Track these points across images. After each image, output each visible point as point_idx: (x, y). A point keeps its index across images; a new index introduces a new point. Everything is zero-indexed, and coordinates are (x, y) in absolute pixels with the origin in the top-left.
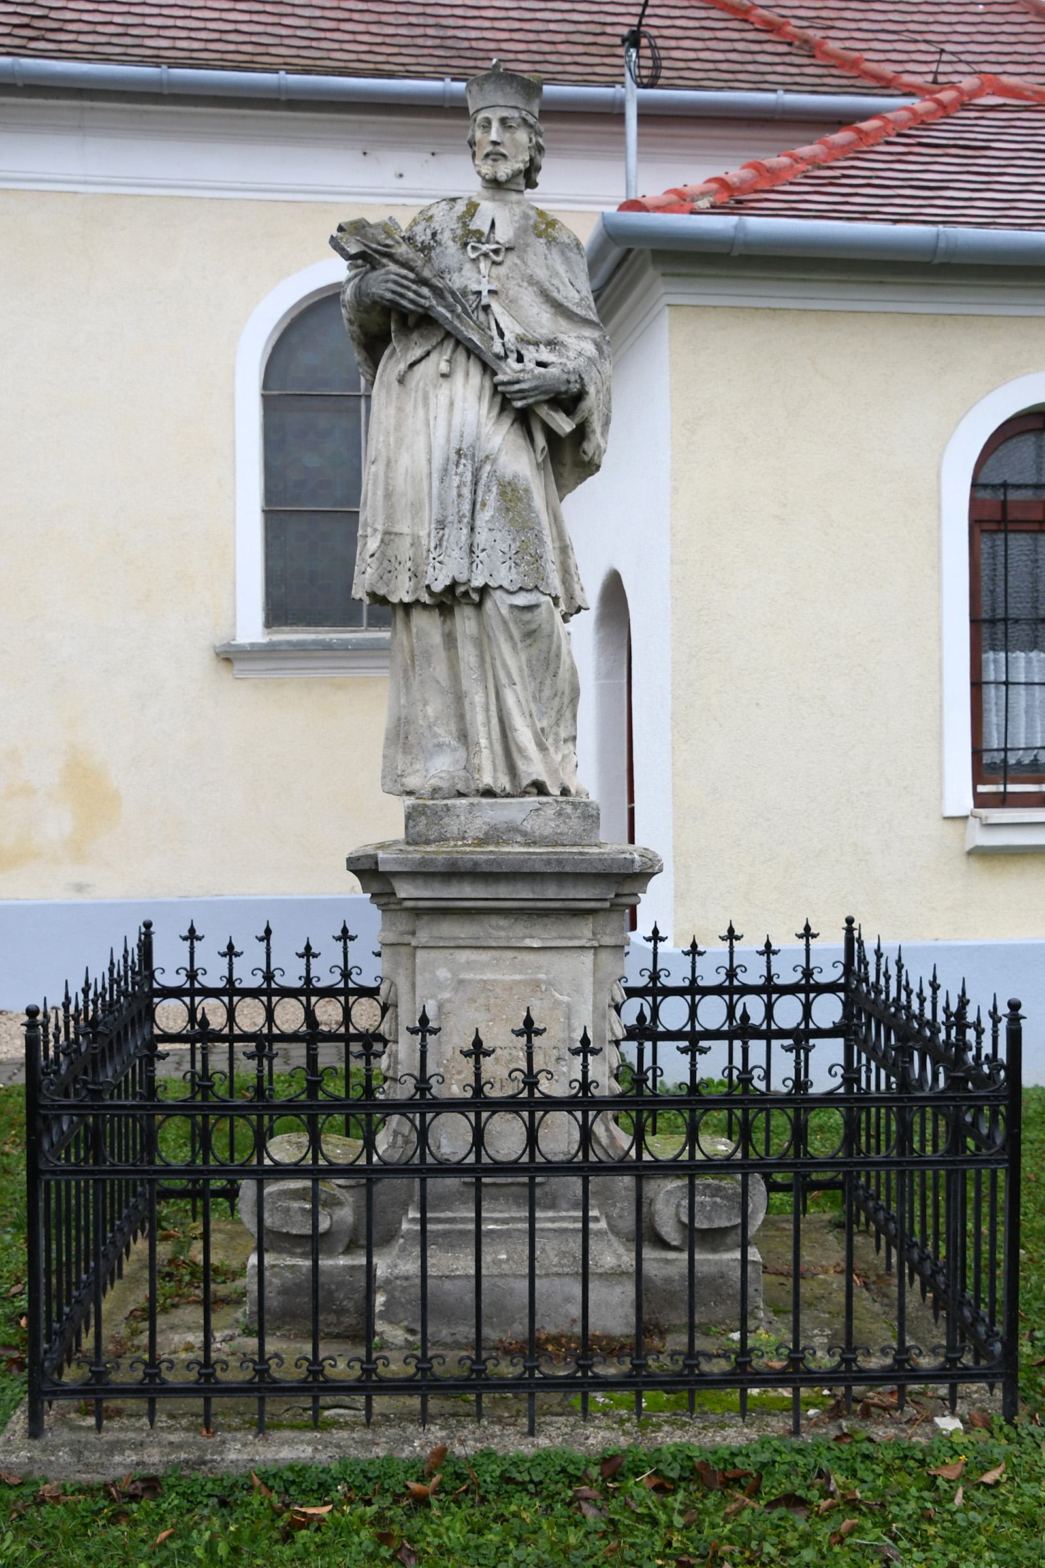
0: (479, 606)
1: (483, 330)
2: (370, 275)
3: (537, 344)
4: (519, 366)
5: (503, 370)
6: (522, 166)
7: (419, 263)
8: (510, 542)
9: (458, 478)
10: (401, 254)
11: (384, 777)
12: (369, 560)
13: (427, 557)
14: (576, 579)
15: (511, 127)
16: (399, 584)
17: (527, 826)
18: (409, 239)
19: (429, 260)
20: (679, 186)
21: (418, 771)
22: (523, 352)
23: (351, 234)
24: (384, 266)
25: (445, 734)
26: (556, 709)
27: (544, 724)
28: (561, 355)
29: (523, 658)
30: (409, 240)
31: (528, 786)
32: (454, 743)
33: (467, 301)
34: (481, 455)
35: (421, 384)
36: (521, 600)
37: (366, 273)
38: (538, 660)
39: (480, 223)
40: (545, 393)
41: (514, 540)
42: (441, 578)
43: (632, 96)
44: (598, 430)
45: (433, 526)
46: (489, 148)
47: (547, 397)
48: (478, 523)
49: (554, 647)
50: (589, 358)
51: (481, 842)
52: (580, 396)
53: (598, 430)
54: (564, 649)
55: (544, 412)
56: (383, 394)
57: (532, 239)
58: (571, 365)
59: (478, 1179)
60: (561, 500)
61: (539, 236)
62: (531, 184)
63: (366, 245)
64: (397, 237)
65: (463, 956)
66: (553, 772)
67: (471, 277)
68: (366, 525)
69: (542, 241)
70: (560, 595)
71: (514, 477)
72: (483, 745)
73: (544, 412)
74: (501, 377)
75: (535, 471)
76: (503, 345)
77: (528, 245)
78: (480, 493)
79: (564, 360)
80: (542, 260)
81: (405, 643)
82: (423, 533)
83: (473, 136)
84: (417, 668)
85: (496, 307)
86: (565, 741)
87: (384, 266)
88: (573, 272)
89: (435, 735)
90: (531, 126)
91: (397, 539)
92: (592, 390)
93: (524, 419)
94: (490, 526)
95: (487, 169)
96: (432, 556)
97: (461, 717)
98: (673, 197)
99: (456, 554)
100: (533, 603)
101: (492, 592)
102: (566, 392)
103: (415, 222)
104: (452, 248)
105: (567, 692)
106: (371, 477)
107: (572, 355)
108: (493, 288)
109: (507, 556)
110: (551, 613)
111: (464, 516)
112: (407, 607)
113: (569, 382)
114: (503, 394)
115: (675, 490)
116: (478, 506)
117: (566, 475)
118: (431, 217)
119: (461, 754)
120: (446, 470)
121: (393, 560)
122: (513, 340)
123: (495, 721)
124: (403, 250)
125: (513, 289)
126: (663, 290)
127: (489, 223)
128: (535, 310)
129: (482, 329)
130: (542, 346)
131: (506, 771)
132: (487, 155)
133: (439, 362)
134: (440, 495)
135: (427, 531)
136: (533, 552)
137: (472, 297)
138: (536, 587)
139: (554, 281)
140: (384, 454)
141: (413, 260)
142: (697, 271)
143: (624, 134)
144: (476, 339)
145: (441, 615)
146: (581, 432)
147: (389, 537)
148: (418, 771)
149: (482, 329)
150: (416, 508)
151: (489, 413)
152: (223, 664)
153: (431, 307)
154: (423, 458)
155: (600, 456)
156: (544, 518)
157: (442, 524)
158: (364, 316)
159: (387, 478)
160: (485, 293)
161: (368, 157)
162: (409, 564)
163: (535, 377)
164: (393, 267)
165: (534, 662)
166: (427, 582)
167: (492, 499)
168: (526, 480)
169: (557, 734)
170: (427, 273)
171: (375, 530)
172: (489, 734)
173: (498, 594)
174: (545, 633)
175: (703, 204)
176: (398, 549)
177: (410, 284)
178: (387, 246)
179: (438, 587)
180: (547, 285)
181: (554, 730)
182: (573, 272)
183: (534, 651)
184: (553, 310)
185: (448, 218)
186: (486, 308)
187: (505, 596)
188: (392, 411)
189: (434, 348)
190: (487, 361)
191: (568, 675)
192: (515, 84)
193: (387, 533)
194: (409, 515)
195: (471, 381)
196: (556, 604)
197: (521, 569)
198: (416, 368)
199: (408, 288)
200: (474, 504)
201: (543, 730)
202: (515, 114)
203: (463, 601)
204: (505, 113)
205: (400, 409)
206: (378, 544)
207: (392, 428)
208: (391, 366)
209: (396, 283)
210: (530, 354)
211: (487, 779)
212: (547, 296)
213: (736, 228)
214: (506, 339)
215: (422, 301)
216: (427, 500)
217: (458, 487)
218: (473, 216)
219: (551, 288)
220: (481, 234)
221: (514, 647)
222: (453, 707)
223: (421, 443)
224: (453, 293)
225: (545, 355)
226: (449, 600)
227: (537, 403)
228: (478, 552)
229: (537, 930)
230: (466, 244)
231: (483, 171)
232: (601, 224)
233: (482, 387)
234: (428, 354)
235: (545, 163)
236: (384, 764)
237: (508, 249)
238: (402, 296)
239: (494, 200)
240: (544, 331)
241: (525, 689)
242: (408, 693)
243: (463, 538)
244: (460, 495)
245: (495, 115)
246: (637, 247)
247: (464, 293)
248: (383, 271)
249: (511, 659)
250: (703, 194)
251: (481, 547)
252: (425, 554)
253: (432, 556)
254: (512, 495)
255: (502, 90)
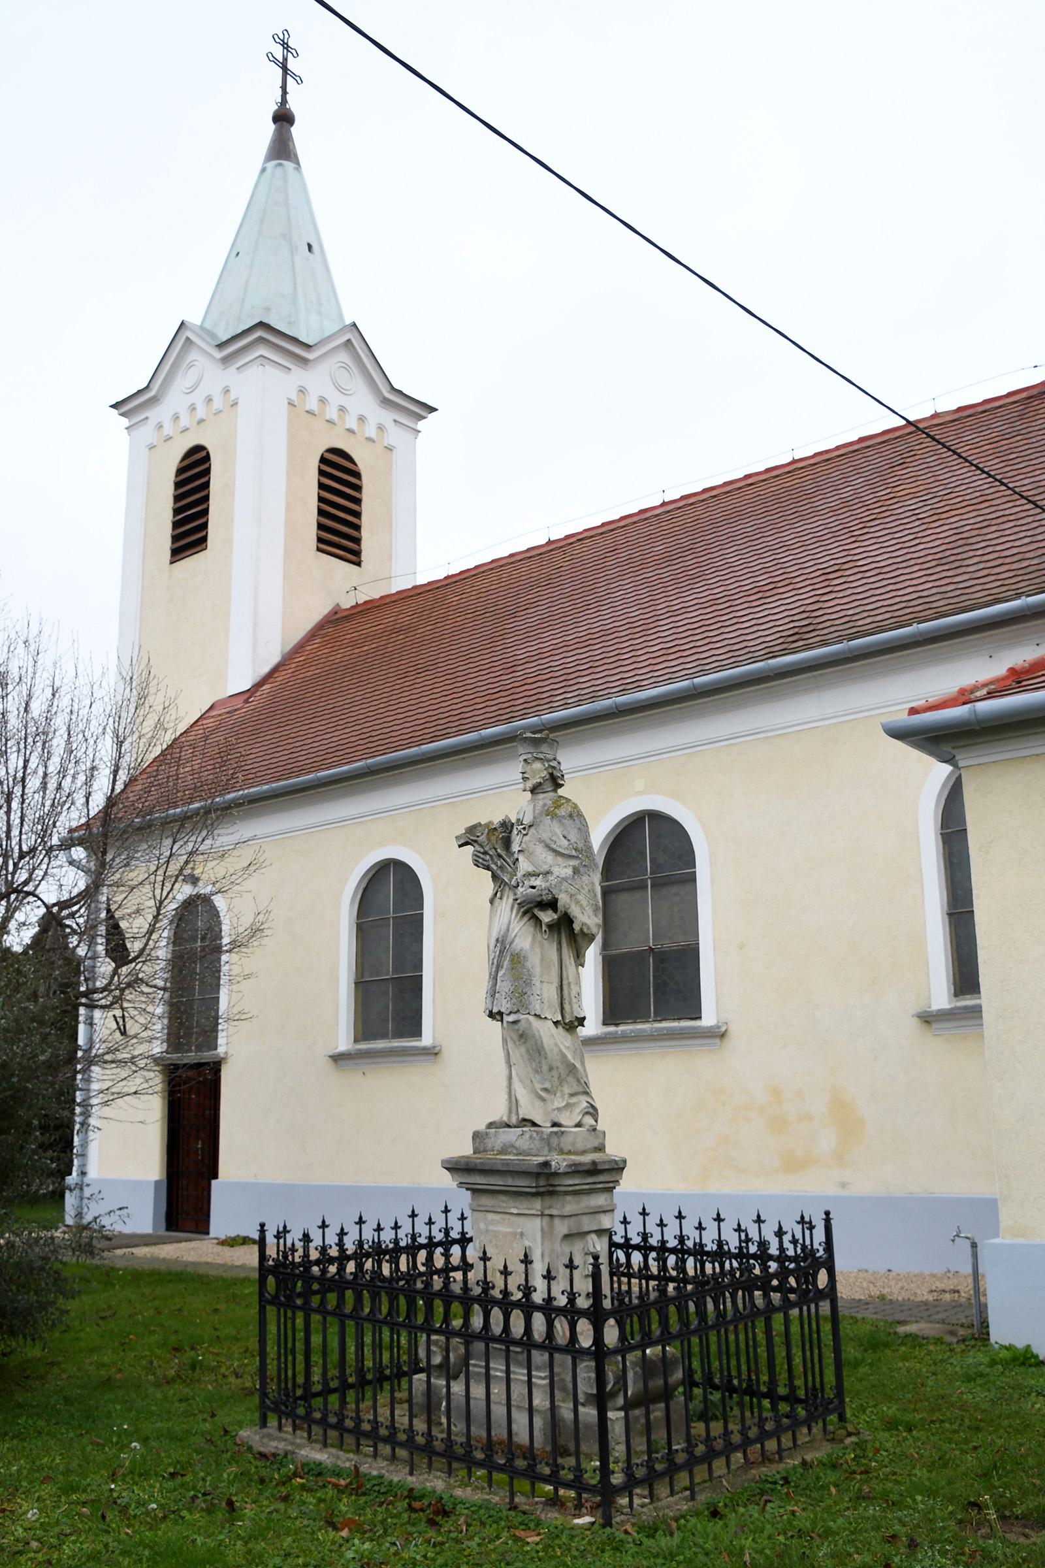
17: (517, 1144)
29: (523, 1049)
36: (511, 1018)
51: (500, 1153)
59: (508, 1348)
65: (490, 1216)
85: (521, 858)
142: (971, 742)
152: (925, 1025)
180: (548, 841)
204: (525, 757)
229: (518, 1204)
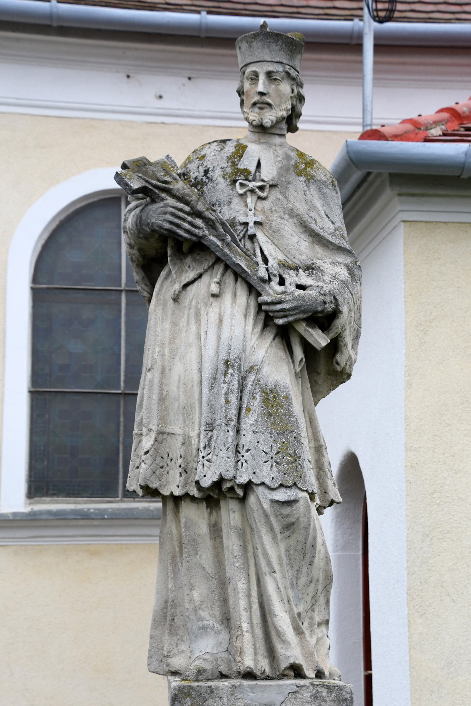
0: (243, 500)
1: (249, 256)
2: (150, 207)
3: (296, 269)
4: (281, 289)
5: (266, 291)
6: (285, 114)
7: (194, 198)
8: (271, 443)
9: (225, 386)
10: (178, 190)
11: (150, 657)
12: (144, 457)
13: (197, 456)
14: (329, 475)
15: (275, 79)
16: (171, 479)
18: (184, 174)
19: (202, 194)
20: (414, 115)
21: (183, 652)
22: (284, 276)
23: (134, 172)
24: (163, 199)
25: (210, 617)
26: (311, 595)
27: (301, 609)
28: (318, 279)
30: (184, 176)
31: (286, 669)
32: (218, 626)
33: (235, 230)
34: (246, 366)
35: (194, 303)
36: (281, 495)
37: (147, 205)
38: (296, 550)
39: (248, 163)
40: (303, 312)
41: (275, 441)
42: (209, 474)
43: (369, 29)
44: (350, 344)
45: (203, 428)
46: (256, 98)
47: (305, 316)
48: (243, 426)
49: (310, 538)
50: (342, 281)
52: (335, 314)
53: (350, 344)
54: (319, 540)
55: (302, 328)
56: (159, 311)
57: (293, 177)
58: (327, 288)
60: (316, 405)
61: (299, 175)
62: (292, 128)
63: (147, 181)
64: (175, 174)
66: (309, 655)
67: (239, 210)
68: (141, 424)
69: (302, 179)
70: (316, 491)
71: (276, 385)
72: (245, 629)
73: (302, 328)
74: (264, 298)
75: (294, 380)
76: (267, 270)
77: (289, 183)
78: (245, 399)
79: (320, 284)
80: (301, 196)
81: (174, 531)
82: (194, 434)
83: (242, 87)
84: (185, 556)
85: (261, 236)
86: (319, 625)
87: (163, 199)
88: (329, 205)
89: (200, 619)
90: (293, 79)
91: (169, 438)
92: (345, 309)
93: (284, 335)
94: (254, 429)
95: (254, 116)
96: (201, 455)
97: (225, 601)
98: (409, 127)
99: (223, 453)
100: (292, 498)
101: (254, 487)
102: (322, 311)
103: (189, 160)
104: (223, 184)
105: (321, 580)
106: (147, 383)
107: (327, 278)
108: (258, 220)
109: (269, 456)
110: (308, 508)
111: (231, 420)
112: (177, 500)
113: (325, 303)
114: (267, 312)
115: (409, 384)
116: (244, 411)
117: (320, 382)
118: (204, 156)
119: (224, 636)
120: (215, 378)
121: (165, 456)
122: (276, 266)
123: (256, 606)
124: (179, 186)
125: (276, 221)
126: (399, 208)
127: (255, 163)
128: (295, 239)
129: (249, 255)
130: (301, 271)
131: (266, 654)
132: (254, 104)
133: (210, 283)
134: (209, 401)
135: (197, 432)
136: (292, 452)
137: (240, 228)
138: (295, 484)
139: (312, 214)
140: (159, 363)
141: (188, 195)
142: (430, 191)
143: (361, 62)
144: (243, 264)
145: (207, 507)
146: (335, 346)
147: (162, 436)
148: (183, 652)
149: (249, 255)
150: (187, 412)
151: (253, 329)
153: (204, 237)
154: (195, 371)
155: (351, 366)
156: (302, 422)
157: (211, 427)
158: (143, 241)
159: (161, 383)
160: (251, 224)
161: (131, 80)
162: (180, 461)
163: (295, 299)
164: (171, 201)
165: (292, 552)
166: (196, 479)
167: (256, 405)
168: (286, 388)
169: (312, 618)
170: (200, 207)
171: (150, 430)
172: (251, 618)
173: (261, 490)
174: (302, 525)
175: (436, 132)
176: (169, 447)
177: (186, 216)
178: (165, 182)
179: (206, 483)
180: (306, 218)
181: (309, 614)
182: (329, 205)
183: (292, 541)
184: (311, 239)
185: (219, 158)
186: (252, 238)
187: (267, 491)
188: (167, 325)
189: (206, 271)
190: (252, 283)
191: (322, 564)
192: (280, 42)
193: (160, 433)
194: (181, 418)
195: (238, 301)
196: (312, 499)
197: (281, 468)
198: (189, 288)
199: (184, 220)
200: (240, 409)
201: (299, 614)
202: (280, 68)
203: (229, 495)
204: (271, 68)
205: (175, 324)
206: (152, 442)
207: (167, 340)
208: (166, 286)
209: (173, 214)
210: (291, 278)
211: (248, 662)
212: (306, 227)
213: (466, 154)
214: (270, 265)
215: (196, 231)
216: (197, 404)
217: (226, 394)
218: (241, 156)
219: (309, 220)
220: (249, 173)
221: (274, 538)
222: (217, 591)
223: (192, 355)
224: (223, 224)
225: (304, 279)
226: (215, 495)
227: (297, 321)
228: (243, 452)
230: (235, 181)
231: (251, 118)
232: (345, 152)
233: (248, 306)
234: (200, 276)
235: (305, 110)
236: (151, 644)
237: (272, 186)
238: (178, 226)
239: (260, 143)
240: (304, 257)
241: (284, 577)
242: (175, 578)
243: (230, 440)
244: (227, 402)
245: (262, 69)
246: (375, 171)
247: (233, 223)
248: (162, 204)
249: (272, 549)
250: (436, 123)
251: (246, 448)
252: (194, 452)
253: (201, 455)
254: (274, 402)
255: (268, 47)
